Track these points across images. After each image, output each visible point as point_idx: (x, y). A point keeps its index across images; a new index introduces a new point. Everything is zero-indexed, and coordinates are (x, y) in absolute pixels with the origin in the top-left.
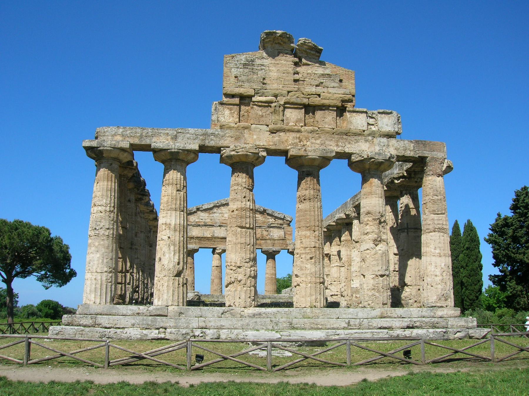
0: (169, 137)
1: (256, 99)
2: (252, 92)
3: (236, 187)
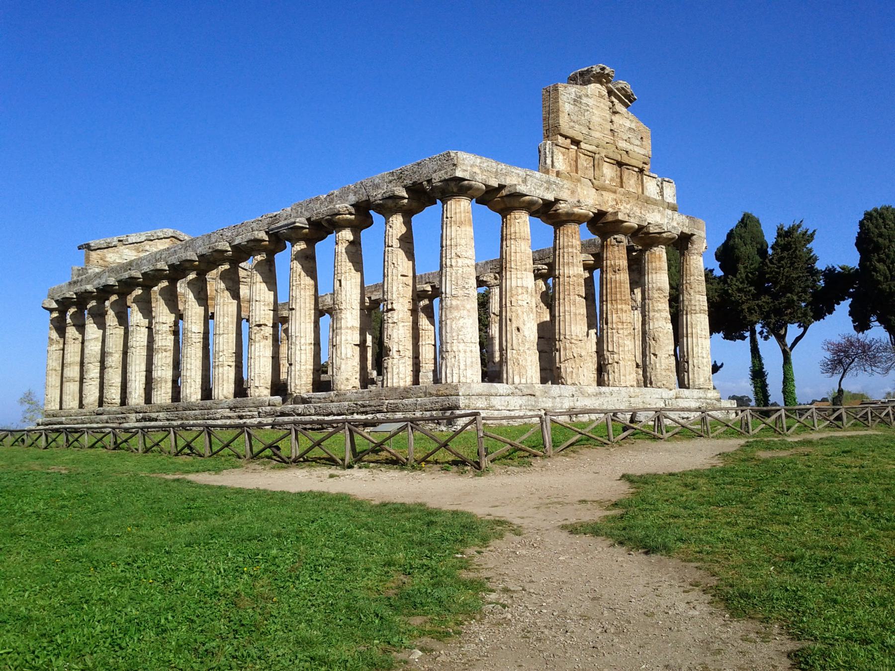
0: (520, 180)
1: (583, 145)
2: (579, 137)
3: (570, 250)
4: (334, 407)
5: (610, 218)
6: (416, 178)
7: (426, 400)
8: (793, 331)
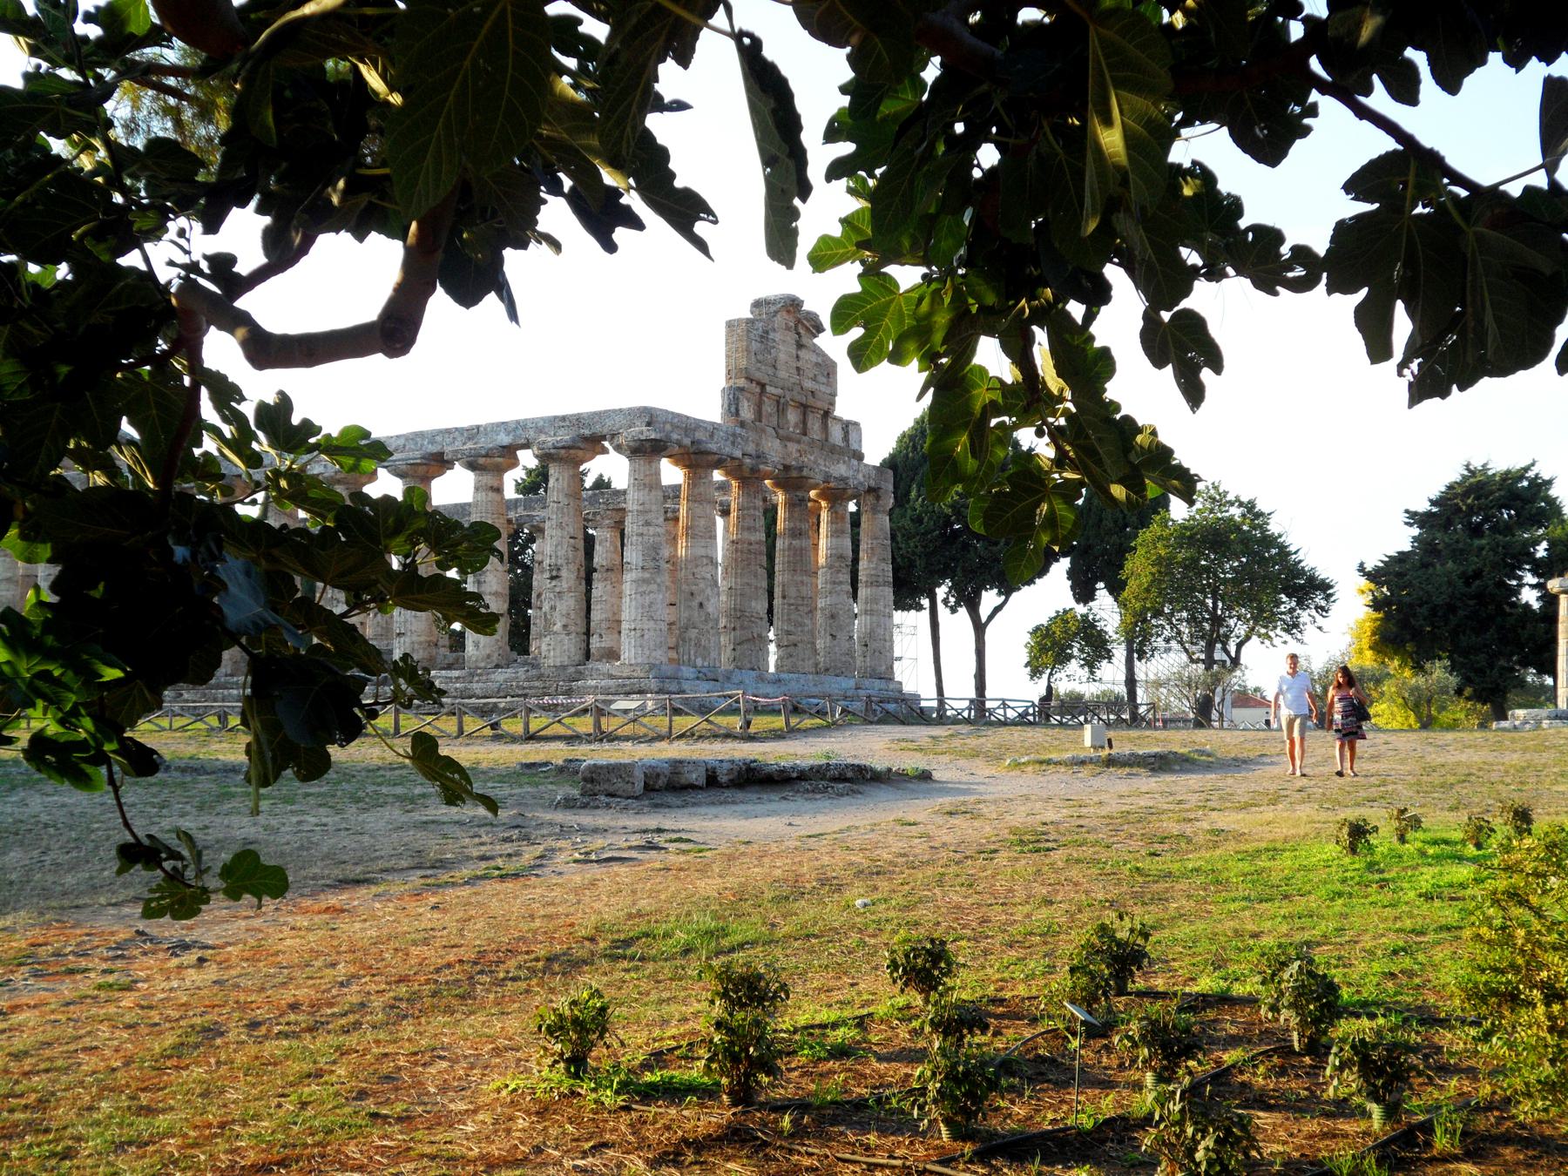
1: (768, 388)
2: (765, 380)
4: (477, 687)
5: (794, 474)
6: (598, 429)
7: (612, 682)
8: (989, 599)
